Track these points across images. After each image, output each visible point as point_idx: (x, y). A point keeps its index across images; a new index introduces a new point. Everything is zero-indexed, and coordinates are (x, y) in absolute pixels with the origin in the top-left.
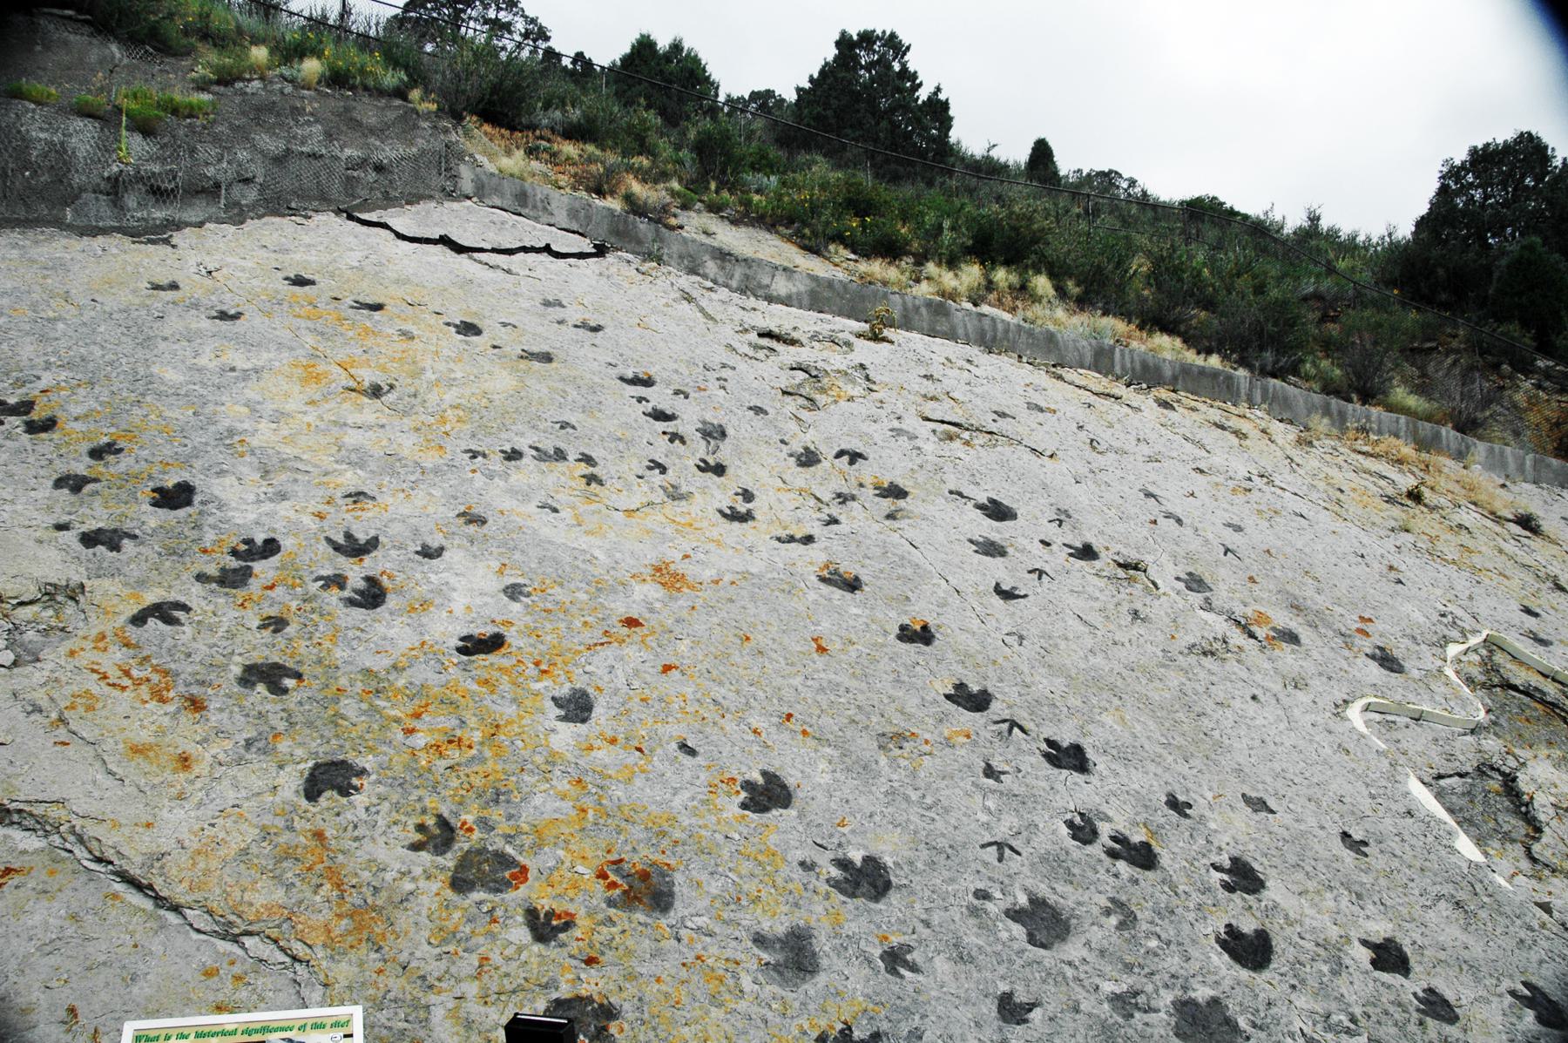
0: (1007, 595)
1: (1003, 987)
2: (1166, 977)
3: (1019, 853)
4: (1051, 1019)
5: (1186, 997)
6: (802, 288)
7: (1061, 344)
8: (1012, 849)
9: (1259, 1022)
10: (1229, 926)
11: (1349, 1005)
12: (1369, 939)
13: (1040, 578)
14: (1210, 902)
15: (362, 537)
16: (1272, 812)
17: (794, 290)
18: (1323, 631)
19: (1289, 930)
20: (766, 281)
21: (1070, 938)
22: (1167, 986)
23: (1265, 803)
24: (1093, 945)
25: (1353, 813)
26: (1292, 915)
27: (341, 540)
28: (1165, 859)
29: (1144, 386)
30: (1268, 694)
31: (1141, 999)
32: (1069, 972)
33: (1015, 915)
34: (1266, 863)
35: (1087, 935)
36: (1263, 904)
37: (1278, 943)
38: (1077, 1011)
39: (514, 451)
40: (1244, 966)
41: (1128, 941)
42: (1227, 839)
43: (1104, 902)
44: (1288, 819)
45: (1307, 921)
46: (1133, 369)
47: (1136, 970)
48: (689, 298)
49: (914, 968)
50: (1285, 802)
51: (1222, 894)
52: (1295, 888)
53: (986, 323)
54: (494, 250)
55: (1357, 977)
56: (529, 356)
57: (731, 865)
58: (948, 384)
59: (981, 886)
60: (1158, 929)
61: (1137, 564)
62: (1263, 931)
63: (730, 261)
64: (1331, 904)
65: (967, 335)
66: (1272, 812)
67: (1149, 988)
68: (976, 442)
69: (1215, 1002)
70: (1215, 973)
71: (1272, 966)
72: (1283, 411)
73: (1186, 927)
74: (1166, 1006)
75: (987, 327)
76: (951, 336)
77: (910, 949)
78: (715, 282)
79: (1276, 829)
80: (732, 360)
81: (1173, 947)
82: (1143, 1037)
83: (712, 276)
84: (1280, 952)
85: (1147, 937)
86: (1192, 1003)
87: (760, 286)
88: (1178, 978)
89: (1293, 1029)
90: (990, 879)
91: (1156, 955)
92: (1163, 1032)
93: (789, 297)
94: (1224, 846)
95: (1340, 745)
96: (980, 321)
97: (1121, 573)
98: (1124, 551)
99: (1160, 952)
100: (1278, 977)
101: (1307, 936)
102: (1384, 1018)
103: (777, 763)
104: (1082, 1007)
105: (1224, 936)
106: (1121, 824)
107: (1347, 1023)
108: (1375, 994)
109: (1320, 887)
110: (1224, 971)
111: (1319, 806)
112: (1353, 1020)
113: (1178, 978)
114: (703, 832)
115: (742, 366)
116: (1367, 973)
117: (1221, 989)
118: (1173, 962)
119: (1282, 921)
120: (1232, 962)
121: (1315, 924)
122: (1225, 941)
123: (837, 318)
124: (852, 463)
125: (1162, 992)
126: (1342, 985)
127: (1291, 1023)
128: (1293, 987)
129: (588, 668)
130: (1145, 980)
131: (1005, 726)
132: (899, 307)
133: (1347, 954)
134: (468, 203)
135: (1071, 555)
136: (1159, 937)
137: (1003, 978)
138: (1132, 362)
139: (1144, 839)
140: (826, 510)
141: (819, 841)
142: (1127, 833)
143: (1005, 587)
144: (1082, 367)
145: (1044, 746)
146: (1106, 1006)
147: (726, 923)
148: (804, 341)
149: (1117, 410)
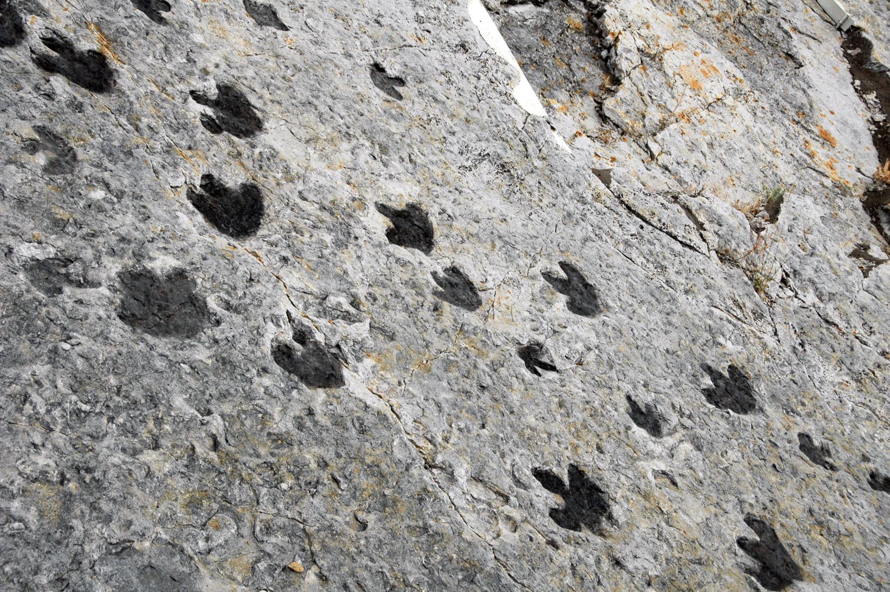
2: (113, 240)
5: (139, 269)
9: (234, 302)
10: (208, 177)
11: (352, 284)
12: (389, 204)
14: (184, 143)
16: (284, 28)
19: (287, 187)
22: (113, 252)
23: (274, 14)
25: (391, 40)
26: (295, 168)
28: (125, 79)
31: (75, 269)
34: (267, 96)
36: (257, 151)
37: (271, 204)
40: (223, 231)
41: (61, 189)
42: (216, 58)
43: (27, 130)
44: (303, 38)
45: (313, 177)
47: (70, 229)
50: (302, 16)
51: (202, 134)
52: (302, 133)
55: (367, 250)
60: (107, 175)
62: (255, 187)
64: (347, 157)
66: (284, 28)
67: (88, 254)
69: (180, 274)
70: (182, 239)
71: (260, 233)
73: (148, 176)
74: (110, 279)
79: (285, 51)
81: (126, 201)
82: (73, 319)
84: (272, 214)
85: (90, 186)
86: (148, 276)
88: (129, 242)
89: (276, 311)
91: (101, 209)
92: (102, 313)
94: (211, 68)
99: (108, 206)
100: (266, 247)
101: (311, 197)
102: (393, 301)
105: (199, 190)
106: (62, 24)
107: (347, 307)
108: (387, 272)
109: (335, 134)
110: (195, 236)
111: (348, 27)
112: (355, 303)
113: (129, 242)
116: (380, 245)
117: (188, 259)
119: (279, 176)
120: (207, 225)
121: (322, 181)
122: (201, 197)
125: (106, 260)
126: (347, 260)
127: (276, 304)
128: (285, 260)
130: (81, 243)
133: (358, 222)
136: (107, 186)
139: (95, 47)
142: (71, 35)
146: (21, 276)
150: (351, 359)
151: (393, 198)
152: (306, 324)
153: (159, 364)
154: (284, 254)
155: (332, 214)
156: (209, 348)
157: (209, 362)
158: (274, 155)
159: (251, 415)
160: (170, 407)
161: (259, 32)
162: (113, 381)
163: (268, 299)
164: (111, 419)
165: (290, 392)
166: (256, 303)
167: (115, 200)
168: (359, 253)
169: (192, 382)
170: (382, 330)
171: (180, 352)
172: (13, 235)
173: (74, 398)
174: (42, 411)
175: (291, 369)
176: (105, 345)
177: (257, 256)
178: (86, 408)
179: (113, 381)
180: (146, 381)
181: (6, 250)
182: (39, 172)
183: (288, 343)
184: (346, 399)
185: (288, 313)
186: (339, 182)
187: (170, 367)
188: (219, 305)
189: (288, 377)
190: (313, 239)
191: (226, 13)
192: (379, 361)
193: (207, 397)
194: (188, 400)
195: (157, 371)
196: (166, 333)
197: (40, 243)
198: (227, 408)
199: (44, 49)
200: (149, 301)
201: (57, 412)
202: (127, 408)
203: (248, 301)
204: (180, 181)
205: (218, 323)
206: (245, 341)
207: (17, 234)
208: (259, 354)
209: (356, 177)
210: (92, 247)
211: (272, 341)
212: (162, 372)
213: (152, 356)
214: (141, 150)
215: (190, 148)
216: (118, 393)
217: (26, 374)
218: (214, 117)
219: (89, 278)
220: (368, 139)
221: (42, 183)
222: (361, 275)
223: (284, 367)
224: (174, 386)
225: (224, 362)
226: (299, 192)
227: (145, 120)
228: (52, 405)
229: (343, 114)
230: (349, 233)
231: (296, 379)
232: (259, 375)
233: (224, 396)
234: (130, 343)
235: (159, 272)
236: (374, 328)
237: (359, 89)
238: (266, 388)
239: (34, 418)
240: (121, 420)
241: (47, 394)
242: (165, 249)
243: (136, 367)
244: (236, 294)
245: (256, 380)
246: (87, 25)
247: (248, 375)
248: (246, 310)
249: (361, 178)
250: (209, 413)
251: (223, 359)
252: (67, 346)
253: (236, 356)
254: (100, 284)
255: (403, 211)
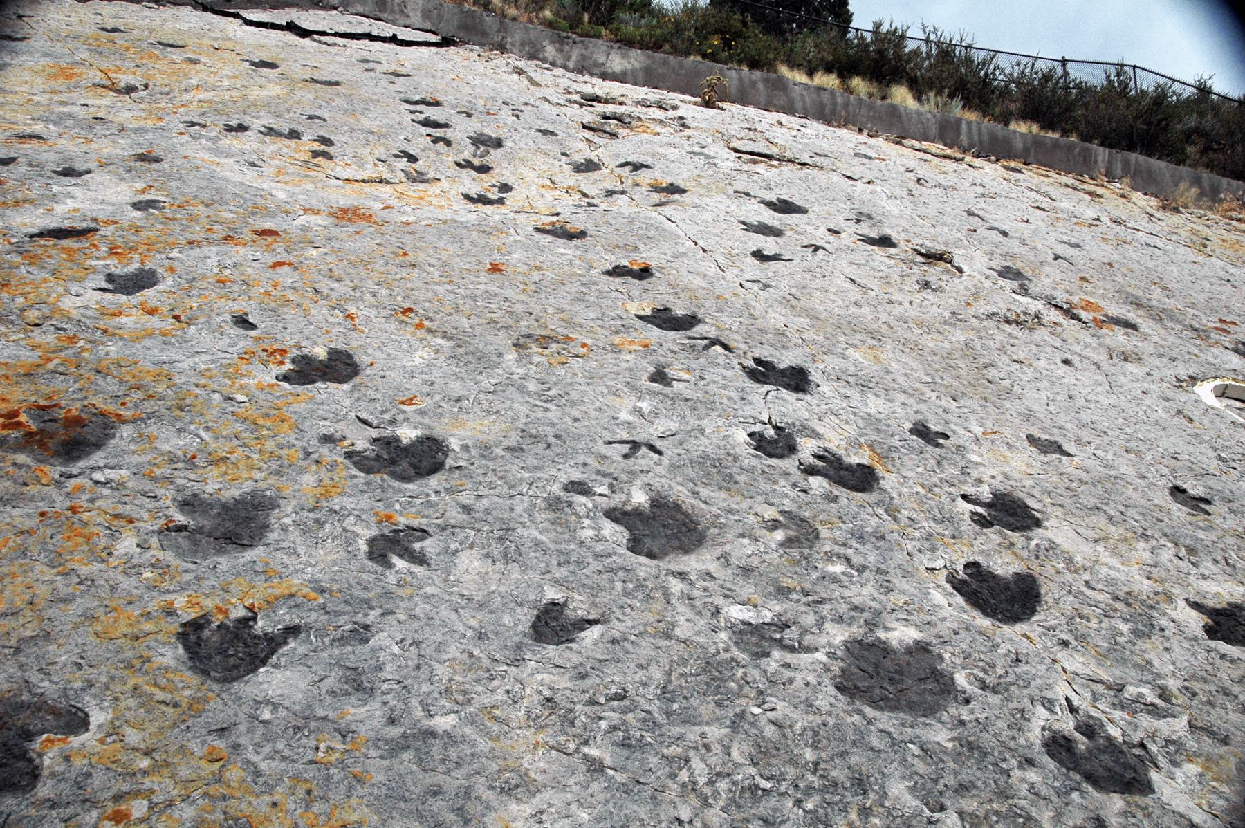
1: (552, 594)
4: (614, 641)
5: (870, 639)
7: (904, 118)
9: (990, 680)
11: (1159, 676)
12: (1205, 602)
14: (947, 533)
18: (1170, 325)
19: (1069, 577)
21: (702, 550)
22: (839, 619)
23: (1060, 447)
24: (733, 561)
25: (1191, 469)
26: (1078, 559)
30: (1086, 361)
31: (791, 634)
32: (676, 586)
35: (728, 548)
36: (1033, 543)
37: (1049, 591)
38: (667, 635)
43: (770, 513)
45: (1103, 571)
46: (981, 142)
48: (520, 72)
49: (420, 559)
52: (1090, 533)
54: (337, 34)
55: (1179, 651)
60: (849, 552)
61: (942, 255)
62: (1031, 576)
64: (1146, 556)
65: (804, 108)
66: (1069, 455)
67: (809, 620)
69: (921, 648)
72: (1145, 182)
74: (830, 645)
75: (825, 101)
76: (789, 110)
77: (424, 533)
82: (773, 683)
83: (551, 59)
84: (1051, 601)
86: (883, 649)
87: (597, 65)
88: (862, 611)
89: (1049, 694)
92: (811, 679)
94: (986, 478)
95: (1179, 412)
96: (819, 95)
98: (927, 243)
102: (1221, 699)
104: (678, 632)
105: (962, 575)
107: (1151, 697)
108: (1209, 668)
112: (1164, 694)
113: (862, 611)
114: (198, 391)
116: (1195, 639)
117: (934, 631)
118: (864, 593)
120: (968, 608)
121: (1113, 574)
122: (964, 581)
125: (828, 626)
126: (1151, 649)
127: (1050, 687)
128: (1065, 644)
130: (803, 608)
132: (735, 82)
133: (1165, 614)
134: (334, 12)
137: (557, 582)
139: (865, 462)
141: (364, 416)
142: (841, 452)
145: (751, 364)
146: (723, 635)
150: (1162, 762)
151: (1209, 596)
152: (1095, 715)
153: (876, 741)
154: (1064, 637)
155: (1128, 605)
156: (951, 730)
157: (950, 745)
158: (1052, 546)
159: (1005, 818)
160: (884, 795)
161: (1042, 457)
162: (809, 755)
163: (1039, 681)
164: (798, 803)
165: (1068, 793)
166: (1021, 683)
167: (855, 574)
168: (1167, 645)
169: (921, 768)
170: (1209, 731)
171: (909, 730)
172: (726, 596)
173: (752, 770)
174: (702, 780)
175: (1071, 765)
176: (807, 712)
177: (1028, 638)
178: (768, 785)
179: (809, 755)
180: (854, 760)
181: (713, 610)
182: (773, 546)
183: (1066, 733)
184: (1158, 812)
185: (1067, 699)
186: (1137, 577)
187: (893, 745)
188: (971, 684)
189: (1066, 775)
190: (1103, 625)
191: (1007, 444)
192: (1207, 768)
193: (941, 787)
194: (912, 789)
195: (872, 749)
196: (896, 708)
197: (755, 606)
198: (970, 805)
199: (812, 460)
200: (878, 674)
201: (722, 785)
202: (822, 790)
203: (1009, 679)
204: (939, 564)
205: (967, 702)
206: (1001, 724)
207: (729, 595)
208: (1022, 741)
209: (1155, 573)
210: (816, 613)
211: (1043, 729)
212: (879, 751)
213: (870, 731)
214: (896, 534)
215: (954, 537)
216: (814, 772)
217: (692, 734)
218: (985, 514)
219: (805, 643)
220: (1171, 541)
221: (776, 555)
222: (1171, 667)
223: (1061, 763)
224: (894, 769)
225: (971, 746)
226: (1086, 582)
227: (905, 513)
228: (719, 774)
229: (1138, 518)
230: (1152, 625)
231: (1078, 777)
232: (1020, 766)
233: (963, 789)
234: (842, 714)
235: (895, 643)
236: (1196, 728)
237: (1156, 502)
238: (1032, 785)
239: (691, 788)
240: (809, 806)
241: (713, 760)
242: (906, 620)
243: (845, 741)
244: (996, 673)
245: (1017, 773)
246: (860, 446)
247: (1004, 766)
248: (1007, 690)
249: (1163, 574)
250: (942, 808)
251: (970, 743)
252: (757, 711)
253: (987, 739)
254: (817, 650)
255: (1224, 609)
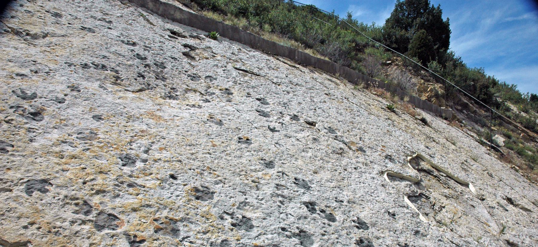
0: (273, 130)
3: (293, 216)
6: (186, 17)
8: (290, 214)
13: (282, 124)
15: (29, 93)
17: (183, 17)
20: (172, 12)
27: (19, 92)
29: (305, 65)
33: (295, 235)
39: (86, 65)
48: (142, 15)
53: (252, 37)
56: (83, 28)
57: (197, 219)
58: (240, 56)
59: (283, 226)
63: (158, 3)
68: (253, 78)
78: (152, 11)
80: (162, 40)
90: (286, 224)
93: (181, 19)
97: (308, 126)
103: (207, 185)
106: (324, 208)
115: (167, 43)
123: (198, 30)
124: (211, 80)
129: (132, 147)
131: (281, 174)
135: (291, 118)
138: (301, 56)
140: (204, 97)
143: (271, 127)
144: (285, 57)
147: (199, 239)
148: (188, 37)
149: (296, 71)
